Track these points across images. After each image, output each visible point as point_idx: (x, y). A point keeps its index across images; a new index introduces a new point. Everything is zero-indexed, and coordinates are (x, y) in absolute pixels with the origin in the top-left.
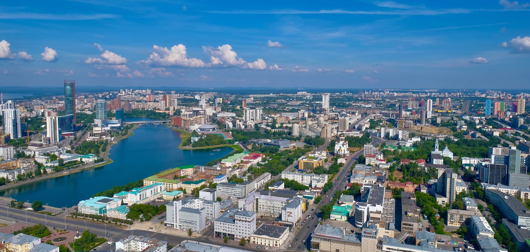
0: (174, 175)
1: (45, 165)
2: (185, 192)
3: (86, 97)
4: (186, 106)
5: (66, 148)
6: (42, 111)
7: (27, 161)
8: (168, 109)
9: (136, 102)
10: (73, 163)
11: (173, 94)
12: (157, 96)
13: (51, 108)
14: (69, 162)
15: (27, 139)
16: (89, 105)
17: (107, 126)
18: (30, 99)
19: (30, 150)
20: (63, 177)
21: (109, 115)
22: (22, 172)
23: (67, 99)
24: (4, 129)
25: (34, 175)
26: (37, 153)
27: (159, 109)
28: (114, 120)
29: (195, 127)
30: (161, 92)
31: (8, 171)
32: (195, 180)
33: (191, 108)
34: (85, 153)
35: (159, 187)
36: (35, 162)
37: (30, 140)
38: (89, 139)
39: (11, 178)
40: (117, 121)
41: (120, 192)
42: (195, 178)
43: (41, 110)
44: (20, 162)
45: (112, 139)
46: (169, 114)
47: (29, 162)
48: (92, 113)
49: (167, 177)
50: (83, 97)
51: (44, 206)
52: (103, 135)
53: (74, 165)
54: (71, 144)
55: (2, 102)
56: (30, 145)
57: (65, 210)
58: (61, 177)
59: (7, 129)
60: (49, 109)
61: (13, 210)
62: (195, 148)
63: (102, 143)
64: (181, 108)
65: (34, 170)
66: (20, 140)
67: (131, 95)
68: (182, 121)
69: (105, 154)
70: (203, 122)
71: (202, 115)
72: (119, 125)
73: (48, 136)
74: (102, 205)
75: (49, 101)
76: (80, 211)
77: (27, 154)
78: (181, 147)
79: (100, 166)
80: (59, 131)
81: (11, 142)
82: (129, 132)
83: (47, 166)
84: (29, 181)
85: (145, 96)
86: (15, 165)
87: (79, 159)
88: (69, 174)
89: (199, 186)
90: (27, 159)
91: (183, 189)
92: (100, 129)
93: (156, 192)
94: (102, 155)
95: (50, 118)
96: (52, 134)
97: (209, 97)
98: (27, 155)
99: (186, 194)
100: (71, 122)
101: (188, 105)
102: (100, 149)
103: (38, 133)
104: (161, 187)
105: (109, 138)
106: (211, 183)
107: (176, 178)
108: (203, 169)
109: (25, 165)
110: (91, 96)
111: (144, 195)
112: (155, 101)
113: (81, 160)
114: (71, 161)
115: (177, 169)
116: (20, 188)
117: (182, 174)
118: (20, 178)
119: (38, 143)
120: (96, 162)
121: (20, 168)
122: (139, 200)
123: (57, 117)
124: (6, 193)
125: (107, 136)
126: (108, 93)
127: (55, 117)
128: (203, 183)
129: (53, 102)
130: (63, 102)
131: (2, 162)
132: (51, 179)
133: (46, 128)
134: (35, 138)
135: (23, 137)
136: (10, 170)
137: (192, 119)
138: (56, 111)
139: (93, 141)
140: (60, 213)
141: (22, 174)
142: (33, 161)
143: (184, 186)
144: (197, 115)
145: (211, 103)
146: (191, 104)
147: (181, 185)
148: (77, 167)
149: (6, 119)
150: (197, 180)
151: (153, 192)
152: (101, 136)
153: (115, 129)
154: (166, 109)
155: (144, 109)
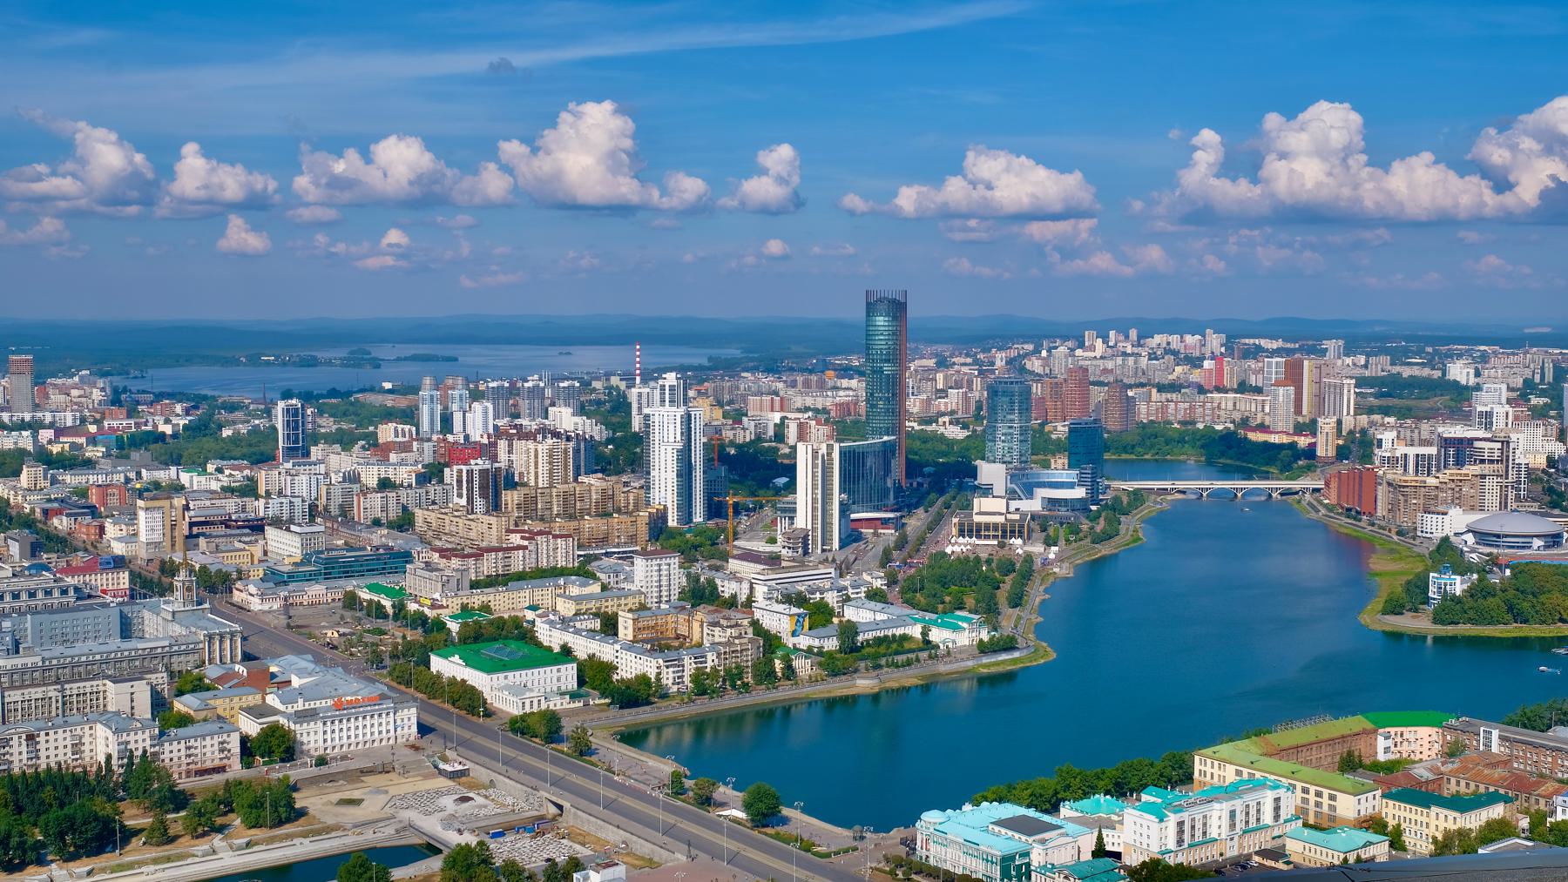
0: (1340, 750)
1: (790, 641)
2: (1396, 842)
3: (943, 363)
4: (1402, 414)
5: (866, 577)
6: (776, 417)
7: (728, 619)
8: (1310, 428)
9: (1154, 391)
10: (894, 646)
11: (1330, 355)
12: (1252, 364)
13: (807, 409)
14: (879, 641)
15: (724, 530)
16: (954, 399)
17: (1030, 495)
18: (731, 368)
19: (734, 577)
20: (850, 701)
21: (1040, 447)
22: (709, 664)
23: (874, 372)
24: (647, 487)
25: (749, 679)
26: (760, 591)
27: (1263, 428)
28: (1060, 469)
29: (1453, 523)
30: (1275, 345)
31: (661, 651)
32: (1451, 788)
33: (1425, 427)
34: (940, 607)
35: (1268, 798)
36: (755, 624)
37: (736, 536)
38: (957, 549)
39: (670, 682)
40: (1070, 475)
41: (1086, 795)
42: (1453, 781)
43: (770, 415)
44: (702, 622)
45: (1052, 556)
46: (1310, 452)
47: (733, 622)
48: (966, 433)
49: (1304, 754)
50: (931, 363)
51: (786, 811)
52: (1013, 532)
53: (897, 653)
54: (883, 565)
55: (638, 379)
56: (734, 557)
57: (862, 838)
58: (847, 697)
59: (657, 486)
60: (799, 410)
61: (676, 807)
62: (1450, 630)
63: (1008, 567)
64: (1372, 424)
65: (749, 657)
66: (700, 532)
67: (1131, 360)
68: (1382, 491)
69: (1019, 618)
70: (1492, 498)
71: (1491, 462)
72: (1080, 493)
73: (802, 521)
74: (1009, 842)
75: (800, 379)
76: (924, 853)
77: (726, 589)
78: (1374, 619)
79: (1000, 669)
80: (841, 503)
81: (668, 538)
82: (1122, 528)
83: (794, 645)
84: (731, 701)
85: (1195, 362)
86: (683, 630)
87: (916, 631)
88: (876, 690)
89: (1474, 821)
90: (727, 612)
91: (1385, 825)
92: (998, 505)
93: (1253, 820)
94: (1009, 619)
95: (810, 448)
96: (814, 517)
97: (1528, 373)
98: (727, 595)
99: (1401, 854)
100: (887, 471)
101: (1409, 409)
102: (1002, 595)
103: (761, 507)
104: (1277, 800)
105: (1037, 548)
106: (1538, 820)
107: (1350, 764)
108: (1494, 739)
109: (720, 635)
110: (962, 360)
111: (1199, 825)
112: (1243, 388)
113: (925, 633)
114: (886, 637)
115: (1356, 723)
116: (700, 725)
117: (1380, 750)
118: (702, 684)
119: (761, 549)
120: (984, 649)
121: (700, 645)
122: (1171, 844)
123: (836, 447)
124: (652, 738)
125: (1028, 539)
126: (1030, 347)
127: (830, 447)
128: (1497, 811)
129: (814, 384)
130: (854, 383)
131: (642, 613)
132: (811, 703)
133: (791, 487)
134: (751, 528)
135: (711, 524)
136: (669, 648)
137: (1431, 481)
138: (827, 422)
139: (972, 557)
140: (846, 851)
141: (708, 670)
142: (745, 622)
143: (1394, 812)
144: (1459, 463)
145: (1535, 401)
146: (1426, 404)
147: (1373, 803)
148: (909, 663)
149: (657, 446)
150: (1463, 789)
151: (1240, 817)
152: (1004, 536)
153: (1063, 512)
154: (1299, 429)
155: (1194, 423)
